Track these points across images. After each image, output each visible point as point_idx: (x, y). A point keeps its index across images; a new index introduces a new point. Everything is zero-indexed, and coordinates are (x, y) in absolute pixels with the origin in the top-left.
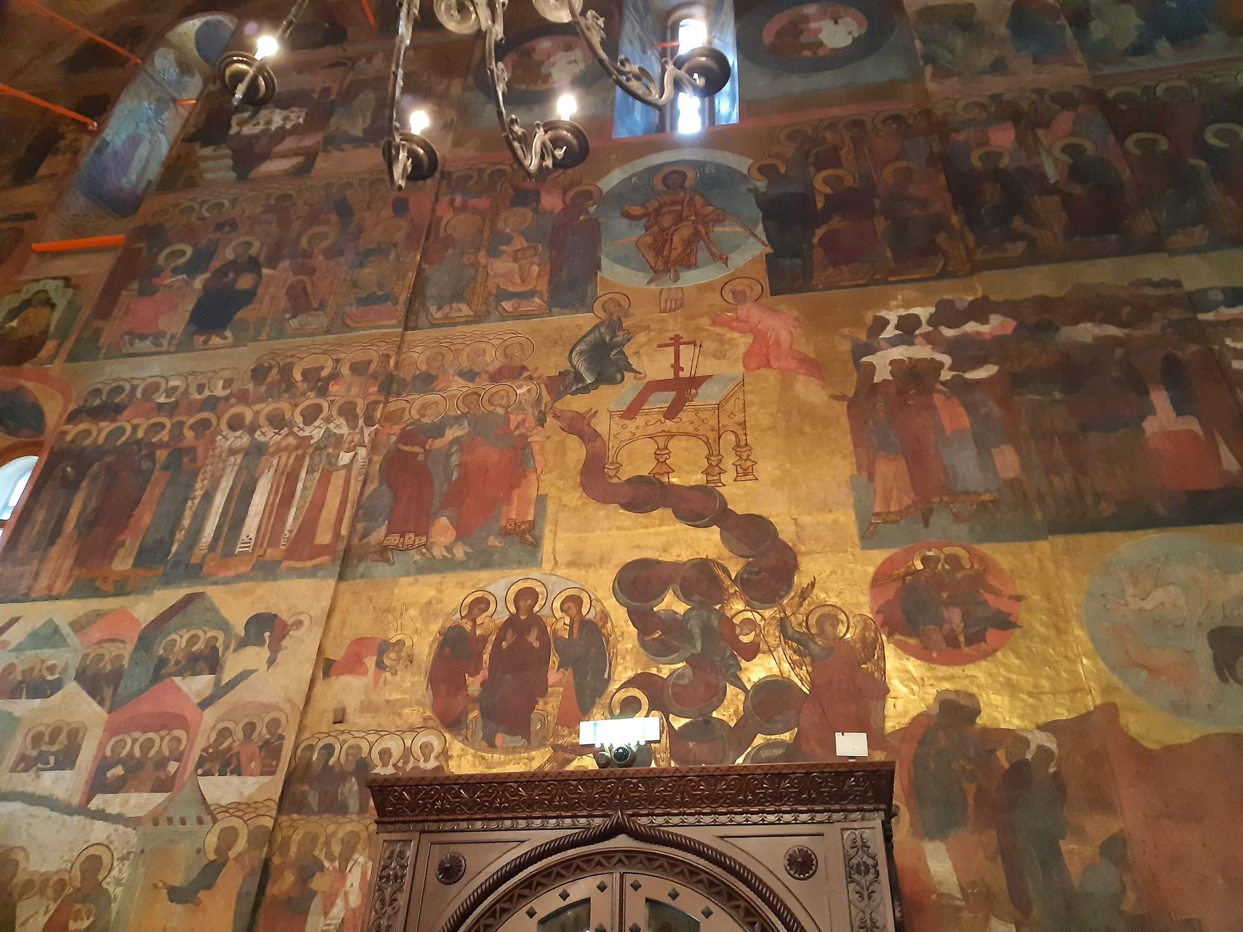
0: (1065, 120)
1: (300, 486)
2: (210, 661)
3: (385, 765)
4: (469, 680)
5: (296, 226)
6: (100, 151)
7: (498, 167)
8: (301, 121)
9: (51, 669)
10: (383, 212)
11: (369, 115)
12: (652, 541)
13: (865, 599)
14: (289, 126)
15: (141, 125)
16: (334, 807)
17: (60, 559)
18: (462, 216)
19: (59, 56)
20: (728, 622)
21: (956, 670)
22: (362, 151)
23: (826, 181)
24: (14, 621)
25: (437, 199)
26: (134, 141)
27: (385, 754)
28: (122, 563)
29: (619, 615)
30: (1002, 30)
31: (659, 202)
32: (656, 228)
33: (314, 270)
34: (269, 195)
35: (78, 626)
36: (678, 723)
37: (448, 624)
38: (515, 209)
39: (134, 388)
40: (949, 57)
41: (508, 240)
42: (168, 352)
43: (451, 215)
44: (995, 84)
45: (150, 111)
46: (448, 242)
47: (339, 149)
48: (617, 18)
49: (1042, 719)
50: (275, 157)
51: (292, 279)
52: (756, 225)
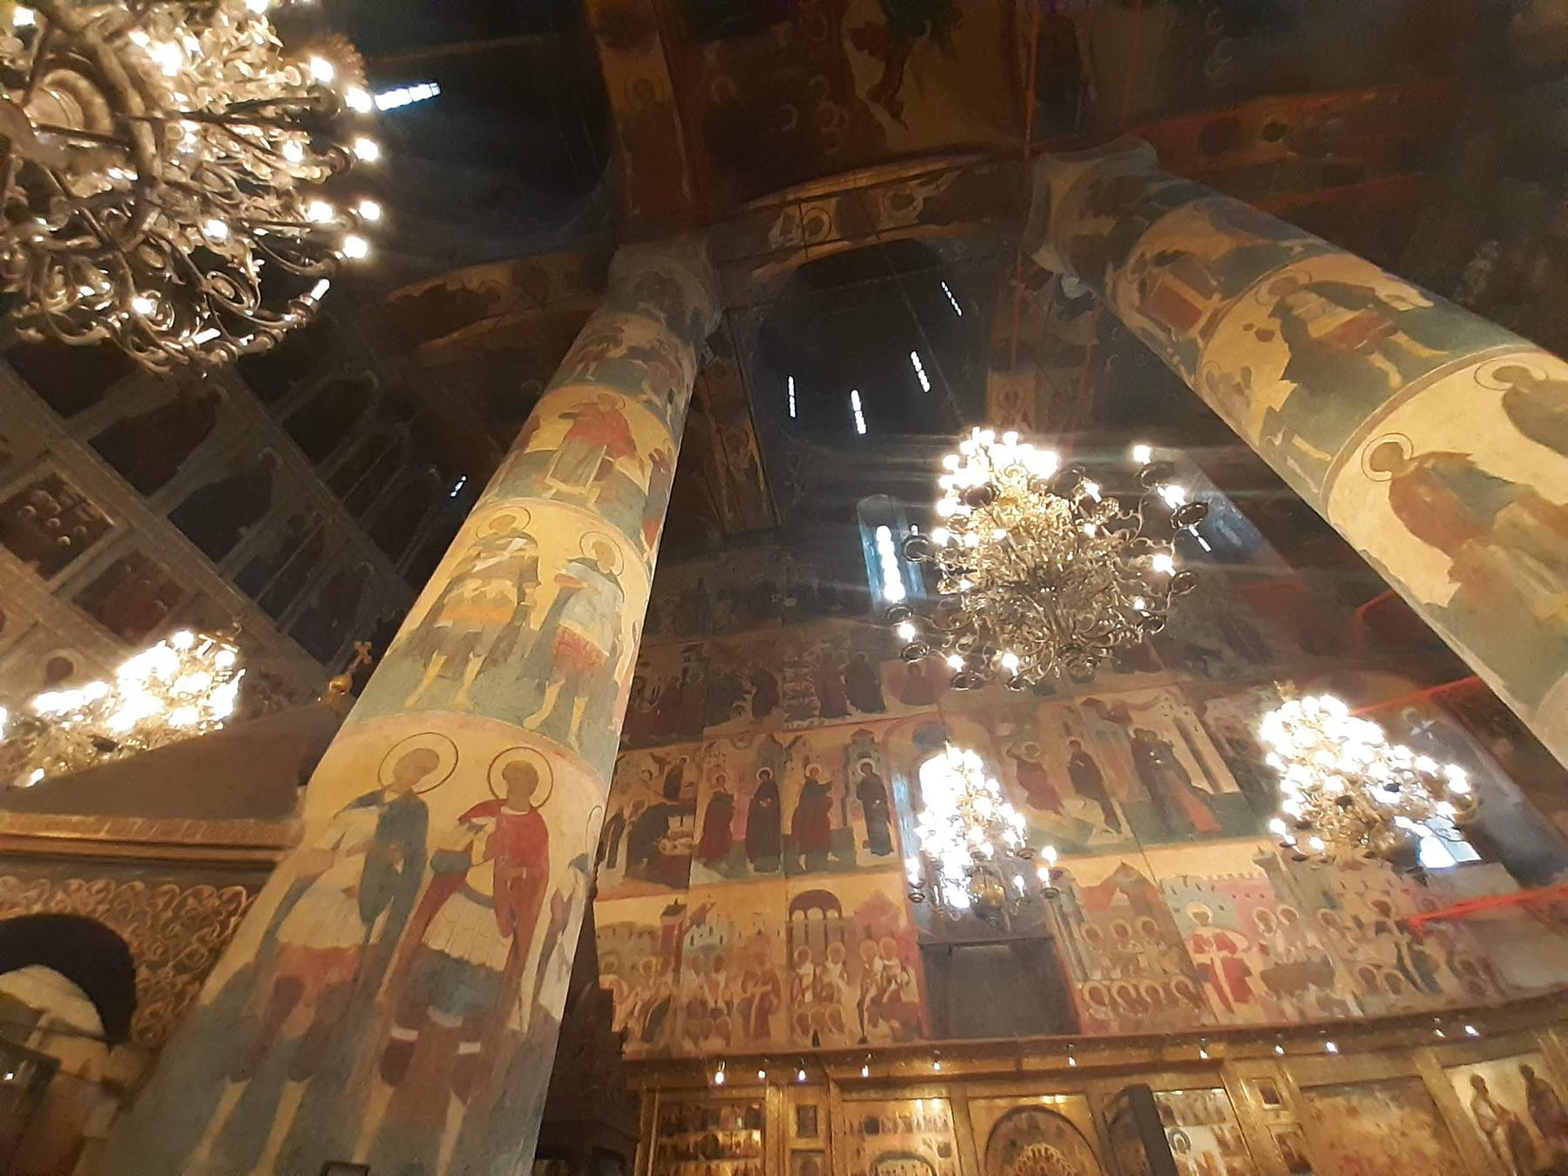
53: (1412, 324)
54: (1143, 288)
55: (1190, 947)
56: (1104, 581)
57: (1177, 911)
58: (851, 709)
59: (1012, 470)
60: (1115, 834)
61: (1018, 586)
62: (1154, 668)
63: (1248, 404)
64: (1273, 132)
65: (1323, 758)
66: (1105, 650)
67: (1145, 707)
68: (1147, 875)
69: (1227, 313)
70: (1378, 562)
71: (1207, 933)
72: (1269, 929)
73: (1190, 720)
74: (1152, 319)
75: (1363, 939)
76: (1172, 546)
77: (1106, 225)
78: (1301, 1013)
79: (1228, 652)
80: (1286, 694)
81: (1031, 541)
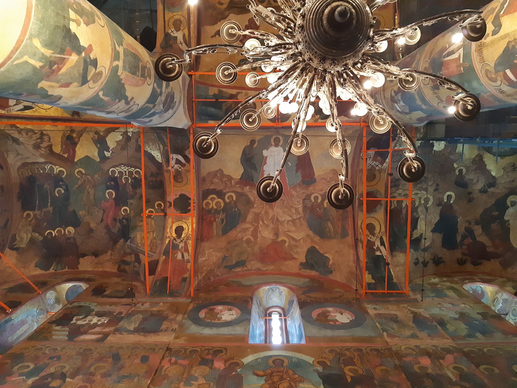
0: (450, 358)
5: (90, 362)
6: (7, 322)
7: (195, 348)
8: (106, 322)
10: (136, 361)
11: (138, 323)
14: (99, 323)
15: (30, 317)
18: (174, 367)
19: (6, 286)
22: (131, 336)
23: (349, 370)
25: (163, 358)
26: (23, 323)
30: (411, 324)
31: (271, 370)
32: (270, 381)
33: (94, 381)
34: (81, 348)
38: (201, 366)
40: (393, 330)
41: (196, 379)
43: (169, 365)
44: (414, 342)
45: (35, 313)
46: (166, 377)
47: (121, 334)
48: (251, 302)
50: (89, 334)
51: (81, 384)
52: (320, 385)
64: (179, 230)
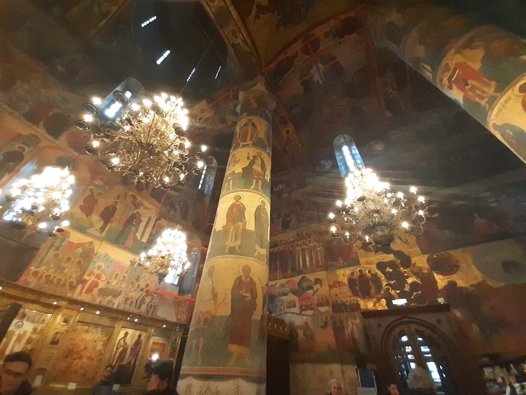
1: (313, 255)
2: (311, 288)
3: (347, 303)
4: (356, 287)
8: (285, 186)
9: (286, 291)
12: (380, 258)
13: (427, 264)
16: (341, 311)
17: (279, 273)
20: (401, 272)
21: (449, 276)
24: (276, 284)
27: (347, 301)
28: (289, 272)
29: (379, 273)
35: (287, 283)
36: (398, 292)
37: (349, 277)
39: (278, 241)
42: (280, 234)
49: (471, 284)
53: (263, 181)
54: (246, 124)
55: (87, 273)
56: (163, 165)
57: (94, 262)
58: (41, 124)
59: (176, 117)
60: (99, 232)
61: (140, 143)
62: (159, 201)
63: (233, 166)
64: (287, 132)
65: (169, 246)
66: (144, 180)
67: (147, 208)
68: (96, 249)
69: (249, 147)
70: (217, 215)
71: (96, 272)
72: (115, 279)
73: (154, 220)
74: (240, 132)
75: (135, 291)
76: (187, 173)
77: (255, 105)
78: (101, 302)
79: (178, 211)
80: (178, 228)
81: (159, 138)
